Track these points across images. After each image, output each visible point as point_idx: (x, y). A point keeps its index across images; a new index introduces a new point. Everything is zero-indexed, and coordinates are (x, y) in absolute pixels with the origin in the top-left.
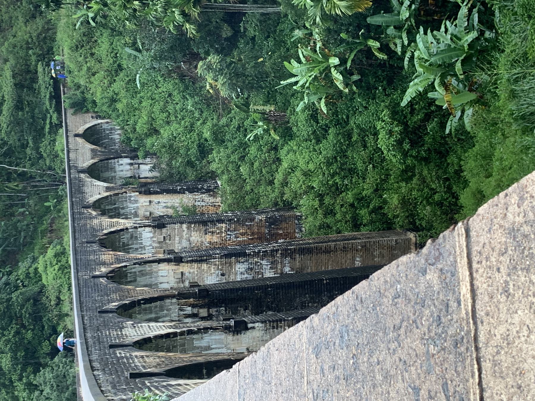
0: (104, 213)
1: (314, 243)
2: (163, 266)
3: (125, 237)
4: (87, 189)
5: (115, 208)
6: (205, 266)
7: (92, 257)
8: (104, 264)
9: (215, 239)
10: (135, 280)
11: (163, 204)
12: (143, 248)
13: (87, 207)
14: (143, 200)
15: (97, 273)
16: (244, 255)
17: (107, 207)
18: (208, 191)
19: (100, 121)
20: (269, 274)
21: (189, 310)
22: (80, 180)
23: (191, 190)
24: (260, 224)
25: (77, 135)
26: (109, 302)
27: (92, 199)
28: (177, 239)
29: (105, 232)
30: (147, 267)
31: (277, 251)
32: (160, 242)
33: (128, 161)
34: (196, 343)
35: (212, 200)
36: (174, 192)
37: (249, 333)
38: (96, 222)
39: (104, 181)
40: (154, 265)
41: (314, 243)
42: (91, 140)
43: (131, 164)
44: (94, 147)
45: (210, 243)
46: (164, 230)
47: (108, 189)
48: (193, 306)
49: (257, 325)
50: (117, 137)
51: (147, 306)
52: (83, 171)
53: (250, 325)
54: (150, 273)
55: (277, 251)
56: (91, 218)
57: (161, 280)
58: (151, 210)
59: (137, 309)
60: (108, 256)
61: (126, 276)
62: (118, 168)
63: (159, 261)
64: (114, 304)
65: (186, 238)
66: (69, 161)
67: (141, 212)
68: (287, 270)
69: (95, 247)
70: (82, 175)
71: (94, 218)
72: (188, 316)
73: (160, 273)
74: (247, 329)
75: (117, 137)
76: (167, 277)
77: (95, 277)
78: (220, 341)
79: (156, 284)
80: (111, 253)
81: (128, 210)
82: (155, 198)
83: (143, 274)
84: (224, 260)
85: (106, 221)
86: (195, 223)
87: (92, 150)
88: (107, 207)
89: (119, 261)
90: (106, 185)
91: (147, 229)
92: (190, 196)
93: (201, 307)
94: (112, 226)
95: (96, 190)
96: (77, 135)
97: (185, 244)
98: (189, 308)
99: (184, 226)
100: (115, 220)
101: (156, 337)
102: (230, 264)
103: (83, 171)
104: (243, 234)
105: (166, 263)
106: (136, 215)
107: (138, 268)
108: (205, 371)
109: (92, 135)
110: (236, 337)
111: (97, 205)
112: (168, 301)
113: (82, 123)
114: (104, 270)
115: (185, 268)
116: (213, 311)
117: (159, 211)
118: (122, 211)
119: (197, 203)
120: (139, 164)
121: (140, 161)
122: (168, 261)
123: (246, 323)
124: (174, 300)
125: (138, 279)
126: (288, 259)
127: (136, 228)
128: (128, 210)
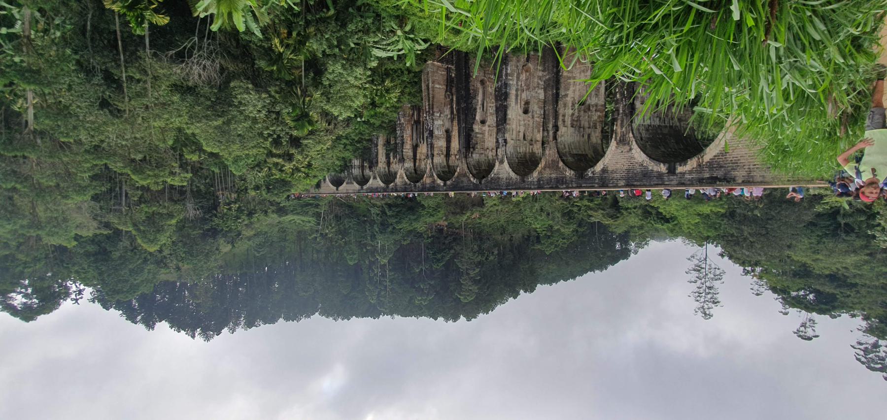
4: (375, 186)
8: (434, 181)
13: (388, 187)
14: (380, 165)
23: (377, 145)
27: (382, 185)
38: (398, 183)
47: (375, 178)
52: (362, 188)
56: (396, 185)
63: (432, 162)
69: (419, 184)
77: (445, 185)
89: (432, 176)
113: (328, 188)
114: (439, 182)
115: (435, 153)
122: (432, 159)
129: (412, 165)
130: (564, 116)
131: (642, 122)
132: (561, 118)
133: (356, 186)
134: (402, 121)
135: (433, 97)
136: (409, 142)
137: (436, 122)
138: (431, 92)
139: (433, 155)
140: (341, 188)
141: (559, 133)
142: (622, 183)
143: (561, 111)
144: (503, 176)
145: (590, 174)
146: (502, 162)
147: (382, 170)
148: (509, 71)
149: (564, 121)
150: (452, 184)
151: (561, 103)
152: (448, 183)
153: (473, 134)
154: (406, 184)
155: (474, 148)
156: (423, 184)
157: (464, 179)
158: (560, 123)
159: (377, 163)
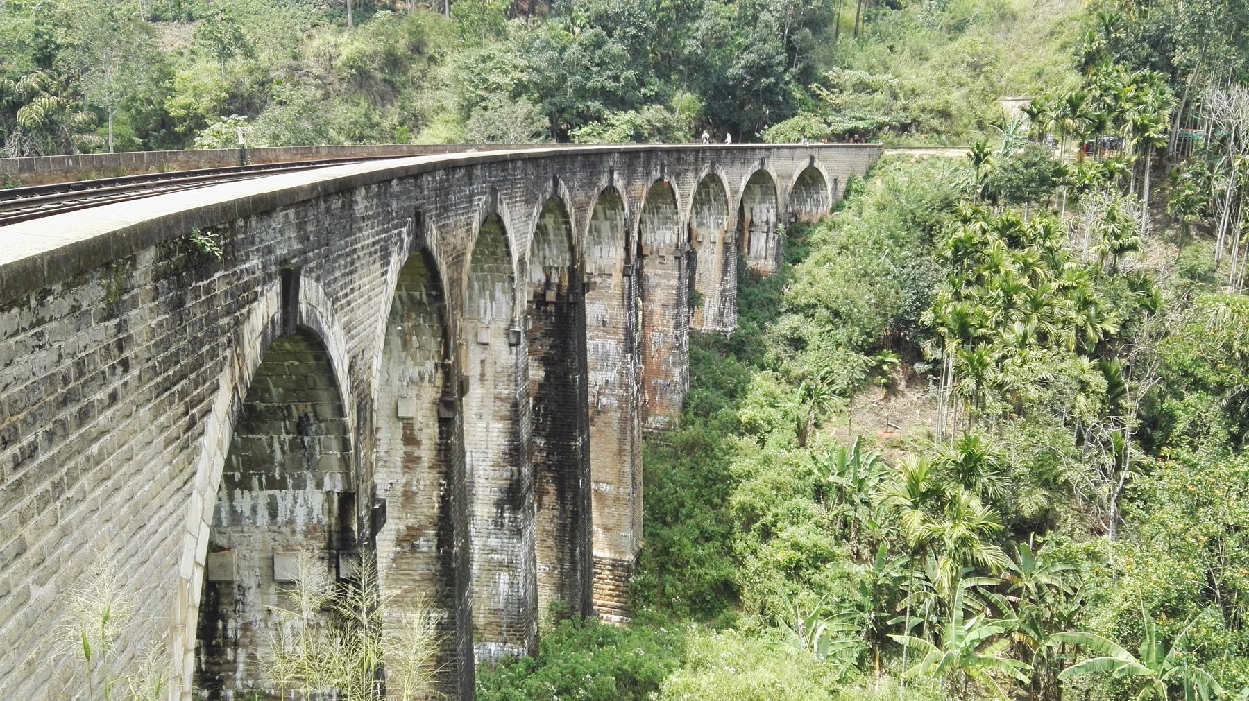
0: (703, 185)
1: (633, 438)
2: (621, 253)
3: (666, 210)
4: (738, 165)
5: (709, 200)
6: (616, 302)
7: (640, 169)
8: (628, 183)
9: (656, 318)
10: (606, 219)
11: (710, 260)
12: (653, 231)
14: (716, 235)
15: (616, 175)
16: (626, 352)
17: (711, 191)
18: (721, 314)
19: (829, 188)
20: (595, 377)
21: (555, 279)
22: (751, 160)
23: (723, 294)
24: (667, 374)
25: (812, 158)
26: (571, 189)
27: (722, 173)
28: (660, 272)
29: (675, 188)
30: (621, 234)
31: (626, 390)
32: (658, 250)
33: (773, 219)
34: (499, 286)
35: (710, 318)
36: (725, 272)
37: (505, 348)
38: (691, 175)
39: (748, 187)
40: (622, 243)
41: (633, 438)
42: (807, 177)
43: (767, 223)
44: (795, 178)
45: (652, 312)
46: (672, 258)
48: (559, 286)
49: (514, 357)
50: (808, 208)
51: (564, 232)
52: (762, 163)
53: (514, 349)
54: (613, 237)
55: (626, 390)
57: (605, 249)
58: (706, 243)
59: (560, 220)
60: (641, 188)
61: (613, 208)
62: (763, 206)
63: (627, 250)
64: (567, 194)
65: (663, 281)
66: (779, 148)
67: (702, 231)
68: (604, 400)
69: (656, 174)
70: (757, 163)
71: (696, 174)
72: (548, 278)
73: (612, 249)
74: (511, 345)
75: (808, 208)
76: (605, 257)
78: (499, 313)
79: (600, 243)
80: (644, 194)
81: (707, 214)
82: (719, 248)
83: (614, 228)
84: (621, 325)
85: (691, 186)
86: (678, 295)
87: (791, 177)
88: (710, 191)
89: (632, 200)
90: (741, 190)
91: (675, 237)
92: (717, 292)
93: (558, 295)
94: (682, 196)
95: (735, 178)
96: (812, 158)
97: (653, 281)
98: (557, 281)
99: (675, 282)
100: (691, 200)
101: (507, 240)
102: (617, 334)
103: (762, 163)
104: (658, 351)
105: (624, 256)
106: (700, 225)
107: (620, 223)
108: (434, 293)
109: (812, 178)
110: (502, 332)
111: (713, 178)
112: (568, 256)
114: (619, 183)
115: (617, 278)
116: (551, 308)
117: (702, 254)
118: (706, 208)
119: (707, 300)
120: (767, 233)
121: (771, 235)
122: (627, 260)
123: (517, 344)
124: (568, 264)
125: (608, 223)
126: (615, 403)
127: (677, 224)
128: (707, 214)
129: (647, 237)
130: (411, 461)
131: (285, 500)
132: (426, 452)
133: (772, 169)
134: (677, 371)
135: (620, 452)
136: (657, 308)
137: (613, 376)
138: (627, 469)
139: (625, 274)
140: (804, 164)
141: (430, 393)
142: (361, 204)
143: (426, 480)
144: (521, 209)
145: (404, 230)
146: (522, 261)
147: (710, 220)
148: (504, 578)
149: (410, 439)
150: (600, 173)
151: (428, 506)
152: (604, 182)
153: (544, 347)
154: (678, 177)
155: (539, 299)
156: (648, 174)
157: (581, 196)
158: (428, 432)
159: (726, 245)
